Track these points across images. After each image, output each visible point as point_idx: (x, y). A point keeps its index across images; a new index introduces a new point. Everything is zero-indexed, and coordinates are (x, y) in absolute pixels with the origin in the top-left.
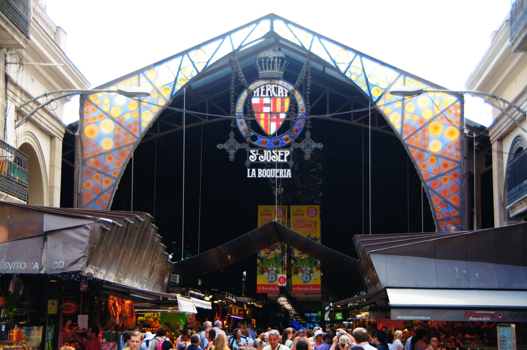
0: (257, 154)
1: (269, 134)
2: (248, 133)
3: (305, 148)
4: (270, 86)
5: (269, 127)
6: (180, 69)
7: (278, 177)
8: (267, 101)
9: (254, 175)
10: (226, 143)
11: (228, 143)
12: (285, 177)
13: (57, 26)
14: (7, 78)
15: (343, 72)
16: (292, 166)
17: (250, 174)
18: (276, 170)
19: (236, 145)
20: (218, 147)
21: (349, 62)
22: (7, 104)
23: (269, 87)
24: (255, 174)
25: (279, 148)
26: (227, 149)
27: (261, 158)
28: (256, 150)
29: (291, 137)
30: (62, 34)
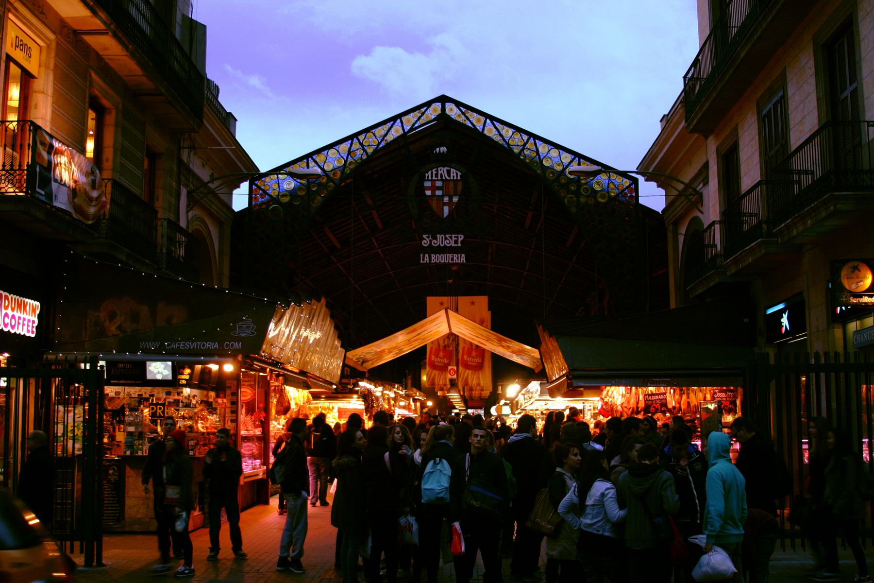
0: (430, 239)
4: (442, 168)
6: (349, 153)
8: (439, 184)
9: (427, 261)
12: (459, 262)
13: (228, 112)
14: (180, 162)
18: (450, 255)
21: (523, 143)
22: (180, 188)
23: (441, 170)
24: (428, 260)
27: (434, 243)
30: (232, 121)
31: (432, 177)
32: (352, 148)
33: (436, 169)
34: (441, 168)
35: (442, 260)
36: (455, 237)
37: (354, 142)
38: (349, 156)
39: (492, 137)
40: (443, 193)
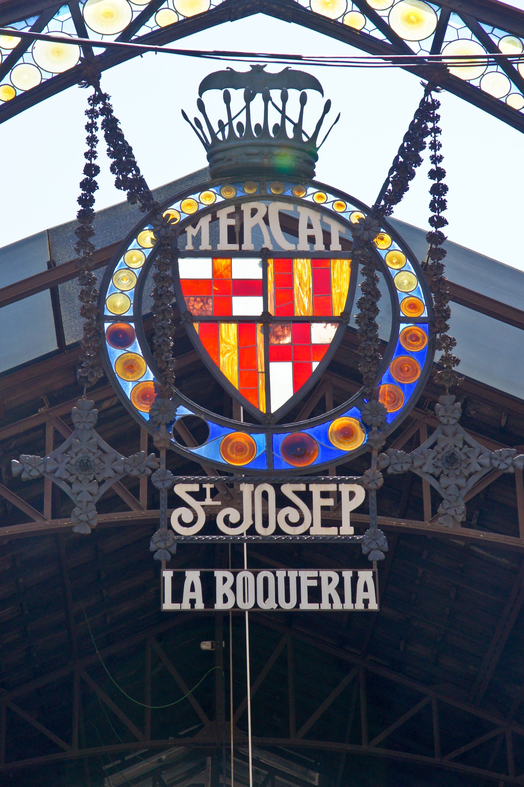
0: (208, 501)
1: (263, 408)
3: (437, 472)
4: (261, 207)
5: (261, 383)
7: (314, 607)
9: (193, 602)
12: (348, 605)
16: (382, 556)
17: (177, 597)
18: (304, 574)
20: (15, 470)
23: (254, 212)
24: (198, 595)
26: (60, 478)
27: (226, 520)
31: (214, 238)
33: (231, 209)
35: (266, 596)
36: (324, 495)
39: (475, 83)
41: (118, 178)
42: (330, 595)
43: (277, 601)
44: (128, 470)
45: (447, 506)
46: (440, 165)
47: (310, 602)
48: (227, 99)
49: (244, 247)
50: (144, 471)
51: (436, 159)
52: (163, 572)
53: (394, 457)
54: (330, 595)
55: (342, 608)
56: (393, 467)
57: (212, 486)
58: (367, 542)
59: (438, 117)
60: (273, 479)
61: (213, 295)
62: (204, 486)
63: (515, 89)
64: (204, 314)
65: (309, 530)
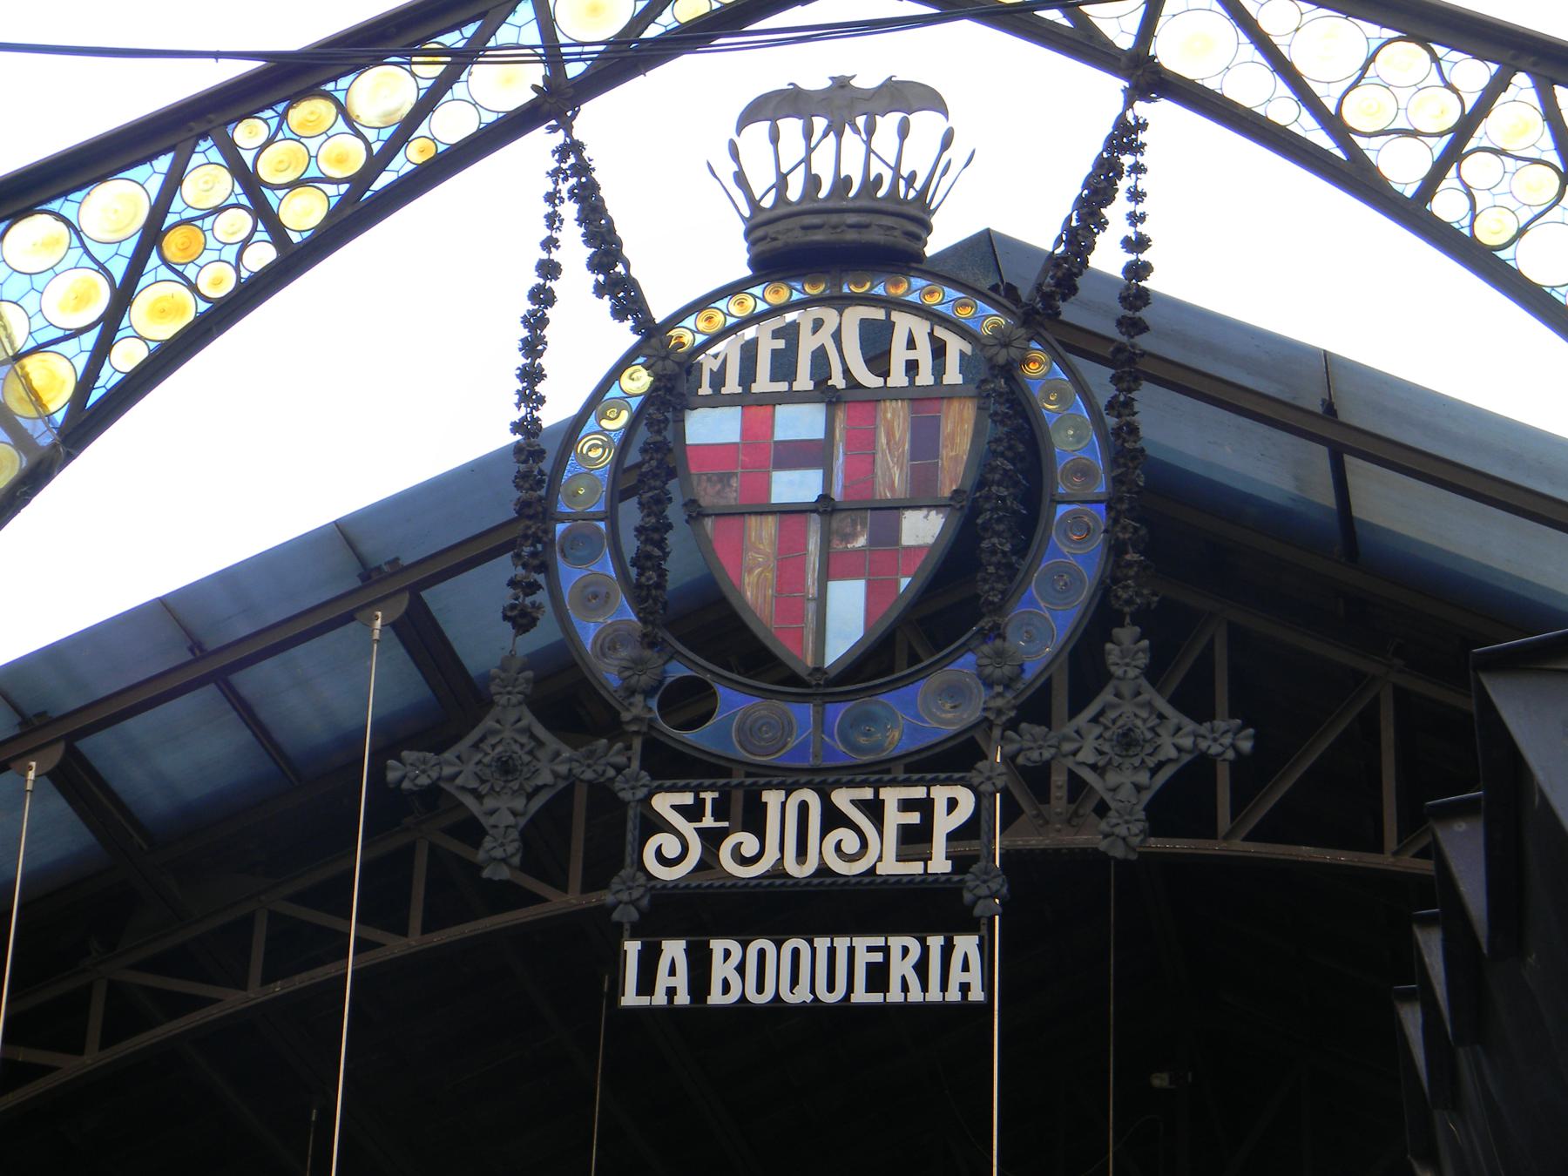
2: (637, 664)
4: (830, 316)
6: (152, 235)
7: (877, 998)
9: (671, 992)
10: (463, 746)
11: (476, 746)
12: (934, 995)
15: (1409, 192)
17: (647, 986)
18: (861, 943)
19: (540, 754)
21: (1452, 117)
23: (818, 325)
24: (681, 981)
25: (879, 773)
26: (463, 788)
28: (697, 792)
29: (988, 683)
31: (748, 375)
32: (177, 205)
34: (816, 312)
35: (795, 981)
36: (906, 805)
37: (196, 159)
38: (154, 256)
39: (1211, 84)
40: (828, 481)
41: (597, 280)
42: (904, 978)
43: (813, 991)
44: (577, 771)
45: (1114, 821)
46: (1141, 228)
47: (868, 991)
48: (775, 138)
49: (797, 386)
50: (604, 772)
51: (1135, 219)
52: (626, 943)
53: (1028, 737)
54: (904, 978)
55: (922, 1000)
56: (1026, 755)
57: (716, 795)
58: (971, 884)
59: (1143, 145)
60: (818, 779)
61: (740, 470)
62: (702, 795)
63: (1283, 89)
64: (722, 502)
65: (874, 867)
